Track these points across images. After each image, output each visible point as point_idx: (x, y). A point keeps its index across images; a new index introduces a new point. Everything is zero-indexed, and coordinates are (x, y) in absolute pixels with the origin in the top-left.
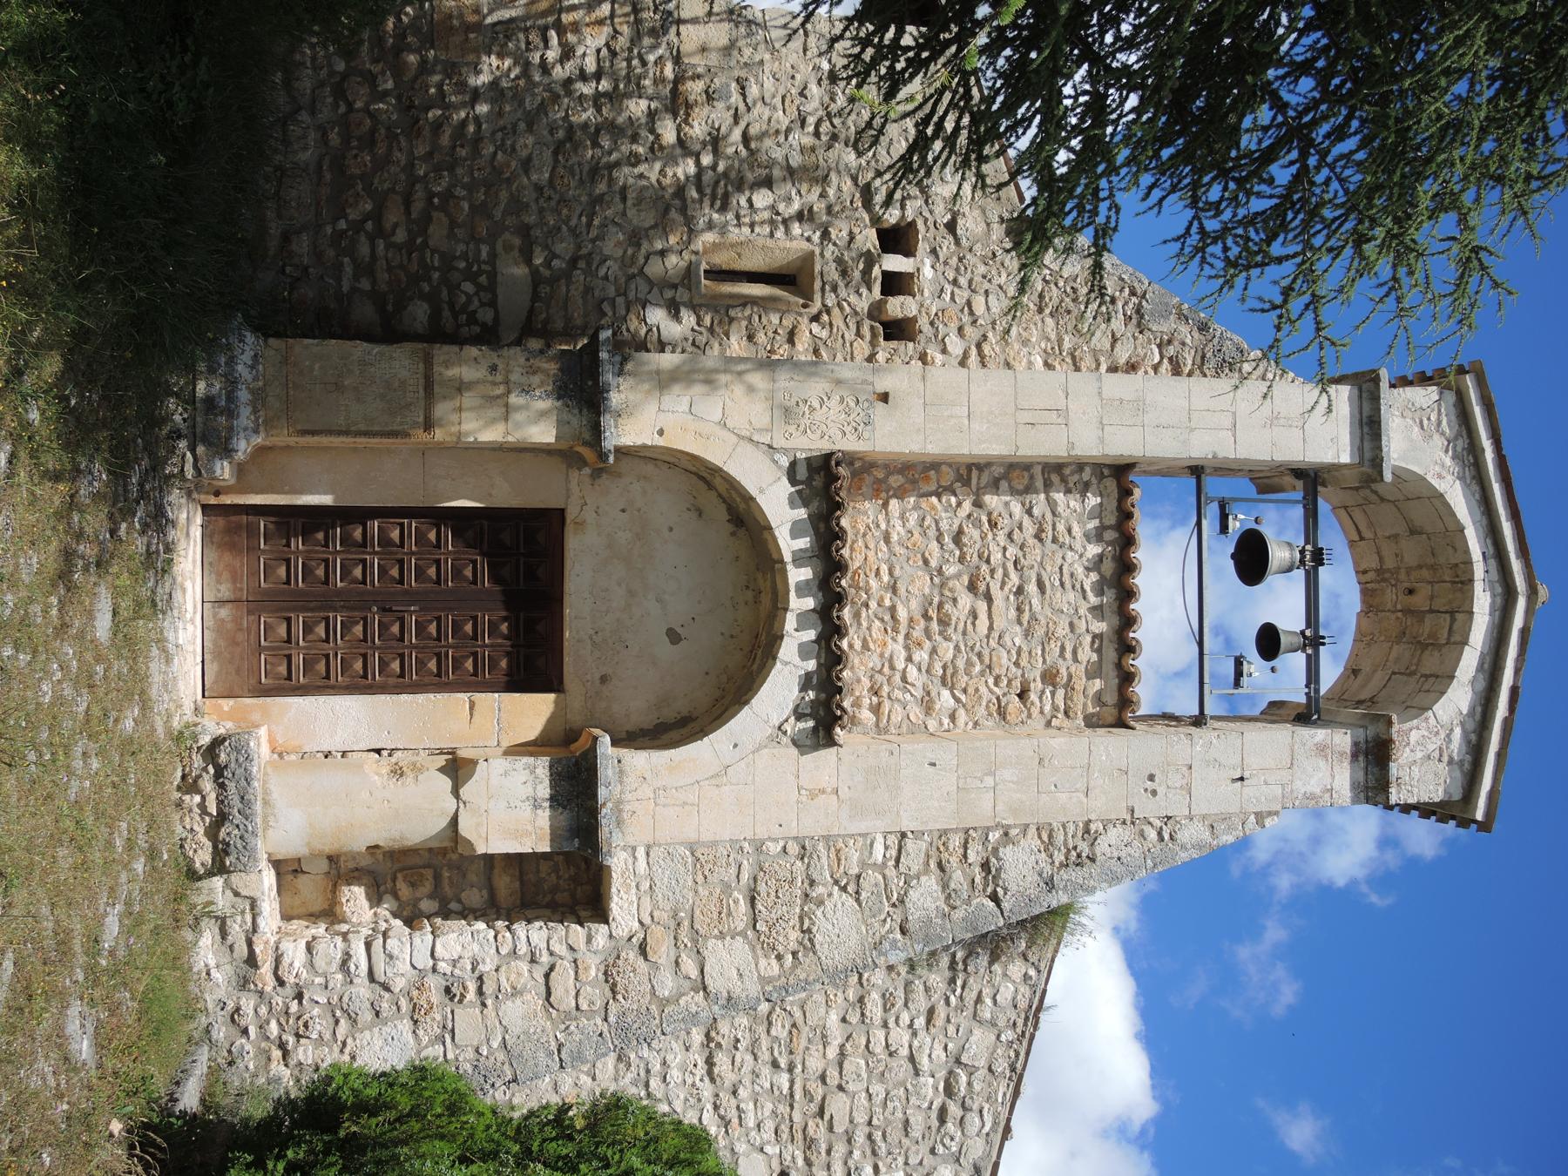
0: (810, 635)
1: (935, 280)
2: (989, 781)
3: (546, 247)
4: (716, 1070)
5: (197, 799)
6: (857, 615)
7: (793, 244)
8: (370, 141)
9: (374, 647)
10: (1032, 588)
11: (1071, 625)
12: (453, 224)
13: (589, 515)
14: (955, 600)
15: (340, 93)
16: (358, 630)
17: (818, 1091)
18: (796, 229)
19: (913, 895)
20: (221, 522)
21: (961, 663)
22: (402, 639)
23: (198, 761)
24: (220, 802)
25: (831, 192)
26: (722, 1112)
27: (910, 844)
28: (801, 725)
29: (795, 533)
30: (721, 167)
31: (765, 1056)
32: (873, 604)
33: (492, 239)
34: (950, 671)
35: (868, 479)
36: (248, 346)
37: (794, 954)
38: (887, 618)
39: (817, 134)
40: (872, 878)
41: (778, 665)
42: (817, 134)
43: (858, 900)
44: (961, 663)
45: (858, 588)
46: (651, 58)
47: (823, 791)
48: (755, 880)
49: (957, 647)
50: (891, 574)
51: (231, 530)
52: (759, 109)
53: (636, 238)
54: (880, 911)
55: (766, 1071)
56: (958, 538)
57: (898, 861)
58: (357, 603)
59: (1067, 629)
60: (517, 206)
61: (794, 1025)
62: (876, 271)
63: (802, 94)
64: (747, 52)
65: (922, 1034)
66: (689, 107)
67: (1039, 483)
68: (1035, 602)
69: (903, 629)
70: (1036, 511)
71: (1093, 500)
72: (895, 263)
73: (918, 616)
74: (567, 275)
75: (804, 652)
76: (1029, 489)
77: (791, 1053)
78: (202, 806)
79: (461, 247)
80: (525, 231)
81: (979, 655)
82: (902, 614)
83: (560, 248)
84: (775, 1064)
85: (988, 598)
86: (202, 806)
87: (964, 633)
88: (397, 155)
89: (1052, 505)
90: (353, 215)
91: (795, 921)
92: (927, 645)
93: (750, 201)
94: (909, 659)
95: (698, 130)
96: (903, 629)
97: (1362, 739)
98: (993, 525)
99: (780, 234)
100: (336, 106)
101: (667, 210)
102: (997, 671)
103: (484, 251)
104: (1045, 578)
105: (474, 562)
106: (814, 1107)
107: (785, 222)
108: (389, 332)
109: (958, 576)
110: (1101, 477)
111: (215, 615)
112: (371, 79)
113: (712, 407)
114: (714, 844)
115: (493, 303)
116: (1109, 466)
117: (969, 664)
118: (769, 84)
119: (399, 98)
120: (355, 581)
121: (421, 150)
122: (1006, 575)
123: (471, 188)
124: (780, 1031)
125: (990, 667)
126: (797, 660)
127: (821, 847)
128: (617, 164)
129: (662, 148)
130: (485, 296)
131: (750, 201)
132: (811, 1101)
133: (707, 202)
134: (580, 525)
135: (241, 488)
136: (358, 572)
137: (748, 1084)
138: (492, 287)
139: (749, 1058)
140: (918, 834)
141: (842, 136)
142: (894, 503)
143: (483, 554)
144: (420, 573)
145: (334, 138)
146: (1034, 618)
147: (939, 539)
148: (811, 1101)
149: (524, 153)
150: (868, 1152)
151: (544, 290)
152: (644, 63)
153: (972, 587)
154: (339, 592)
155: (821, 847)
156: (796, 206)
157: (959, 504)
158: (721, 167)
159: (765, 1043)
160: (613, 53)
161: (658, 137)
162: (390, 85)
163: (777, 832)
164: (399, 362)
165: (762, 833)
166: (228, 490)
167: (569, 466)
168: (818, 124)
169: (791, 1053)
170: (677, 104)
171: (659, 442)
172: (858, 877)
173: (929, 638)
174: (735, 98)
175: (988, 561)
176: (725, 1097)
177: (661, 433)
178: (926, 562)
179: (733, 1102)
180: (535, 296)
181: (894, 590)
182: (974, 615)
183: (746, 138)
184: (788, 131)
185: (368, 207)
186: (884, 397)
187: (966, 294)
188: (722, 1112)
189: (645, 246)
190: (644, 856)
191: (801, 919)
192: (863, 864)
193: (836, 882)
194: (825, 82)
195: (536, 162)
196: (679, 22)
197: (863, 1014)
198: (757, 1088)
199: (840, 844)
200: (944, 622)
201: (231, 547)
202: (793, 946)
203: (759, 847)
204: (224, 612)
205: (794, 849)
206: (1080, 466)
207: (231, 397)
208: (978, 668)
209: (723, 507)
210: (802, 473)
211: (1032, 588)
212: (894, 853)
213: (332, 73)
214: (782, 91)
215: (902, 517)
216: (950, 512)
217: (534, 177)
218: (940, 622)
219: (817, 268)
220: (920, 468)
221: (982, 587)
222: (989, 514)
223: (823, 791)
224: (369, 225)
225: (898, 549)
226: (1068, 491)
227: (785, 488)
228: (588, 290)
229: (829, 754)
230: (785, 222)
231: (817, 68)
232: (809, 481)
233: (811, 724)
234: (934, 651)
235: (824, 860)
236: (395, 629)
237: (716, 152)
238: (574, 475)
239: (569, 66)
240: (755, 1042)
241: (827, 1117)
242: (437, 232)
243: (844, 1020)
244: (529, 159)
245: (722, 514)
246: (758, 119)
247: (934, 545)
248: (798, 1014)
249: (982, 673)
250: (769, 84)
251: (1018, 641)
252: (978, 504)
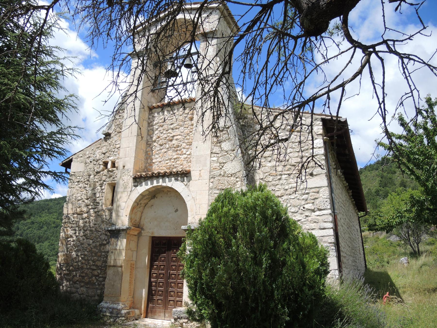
0: (167, 179)
1: (113, 157)
3: (103, 241)
4: (279, 195)
5: (184, 324)
6: (176, 167)
7: (106, 188)
8: (83, 277)
9: (177, 281)
10: (172, 126)
11: (180, 116)
12: (98, 260)
13: (151, 231)
14: (174, 144)
15: (75, 283)
16: (173, 284)
17: (288, 167)
18: (103, 187)
19: (225, 149)
20: (150, 314)
21: (186, 141)
22: (175, 274)
23: (177, 323)
24: (185, 319)
25: (97, 180)
26: (291, 193)
27: (214, 151)
28: (185, 180)
29: (147, 185)
30: (92, 204)
31: (277, 182)
32: (173, 164)
33: (101, 252)
34: (188, 144)
35: (149, 167)
36: (103, 304)
37: (237, 178)
38: (176, 160)
39: (87, 184)
40: (221, 160)
41: (172, 187)
42: (87, 184)
43: (225, 163)
44: (186, 141)
45: (170, 168)
46: (73, 220)
47: (200, 174)
48: (218, 189)
49: (183, 143)
50: (167, 160)
51: (151, 312)
52: (82, 197)
53: (103, 222)
54: (228, 157)
55: (281, 182)
56: (161, 145)
57: (217, 154)
58: (168, 285)
59: (181, 116)
60: (95, 247)
61: (269, 175)
62: (110, 170)
63: (81, 188)
64: (73, 200)
66: (81, 211)
67: (152, 128)
68: (175, 125)
69: (178, 156)
70: (157, 128)
71: (156, 115)
72: (109, 165)
73: (176, 153)
75: (170, 181)
76: (153, 130)
77: (277, 175)
78: (186, 323)
79: (102, 259)
80: (101, 245)
81: (185, 137)
82: (175, 157)
83: (103, 238)
84: (280, 179)
85: (173, 136)
86: (186, 323)
87: (180, 141)
88: (86, 272)
89: (156, 124)
90: (95, 281)
91: (229, 179)
92: (182, 150)
93: (98, 198)
94: (185, 154)
95: (85, 209)
96: (178, 156)
97: (202, 40)
98: (159, 137)
99: (104, 191)
100: (77, 284)
101: (98, 215)
102: (189, 132)
103: (103, 254)
104: (170, 123)
105: (161, 257)
106: (293, 168)
107: (102, 190)
109: (169, 144)
110: (152, 113)
111: (167, 317)
112: (74, 276)
113: (123, 205)
114: (209, 200)
116: (150, 112)
117: (187, 139)
118: (79, 195)
119: (77, 271)
120: (163, 285)
121: (85, 267)
122: (169, 133)
123: (92, 256)
124: (270, 179)
125: (188, 134)
126: (172, 182)
127: (212, 173)
128: (90, 226)
129: (88, 217)
131: (98, 198)
132: (291, 169)
133: (97, 207)
134: (152, 233)
135: (140, 309)
136: (161, 284)
137: (284, 186)
139: (277, 187)
140: (212, 149)
141: (88, 179)
142: (153, 161)
143: (160, 255)
144: (162, 270)
145: (82, 284)
146: (178, 125)
147: (161, 149)
148: (291, 169)
149: (87, 245)
150: (307, 151)
152: (74, 221)
153: (171, 141)
154: (165, 289)
155: (212, 173)
156: (99, 188)
157: (155, 146)
158: (92, 204)
159: (274, 182)
160: (72, 227)
161: (86, 217)
162: (75, 273)
163: (208, 185)
164: (110, 272)
165: (208, 188)
166: (141, 311)
167: (141, 235)
168: (86, 184)
169: (277, 175)
170: (80, 214)
171: (128, 216)
172: (220, 163)
173: (181, 149)
174: (80, 202)
175: (166, 137)
176: (288, 192)
177: (126, 216)
178: (166, 152)
179: (289, 190)
181: (171, 159)
182: (177, 139)
183: (87, 199)
184: (87, 190)
185: (94, 278)
186: (124, 166)
187: (116, 149)
188: (291, 193)
189: (105, 220)
190: (323, 211)
191: (228, 177)
192: (217, 162)
193: (221, 169)
194: (79, 183)
195: (88, 243)
196: (68, 214)
197: (269, 157)
198: (286, 184)
199: (212, 168)
200: (178, 146)
201: (155, 312)
202: (235, 179)
203: (211, 189)
204: (167, 315)
205: (212, 180)
206: (149, 118)
207: (110, 308)
208: (188, 137)
209: (152, 200)
210: (136, 184)
211: (172, 126)
212: (216, 155)
213: (72, 284)
214: (80, 192)
215: (156, 159)
216: (156, 146)
217: (91, 243)
218: (178, 147)
219: (110, 182)
220: (147, 156)
221: (171, 138)
222: (157, 138)
223: (200, 174)
224: (97, 278)
225: (162, 159)
226: (154, 121)
227: (139, 188)
229: (192, 173)
230: (102, 190)
231: (77, 185)
232: (138, 182)
233: (185, 178)
234: (184, 148)
235: (215, 172)
236: (173, 276)
237: (89, 205)
238: (143, 234)
239: (74, 236)
240: (273, 185)
241: (295, 164)
243: (270, 162)
244: (88, 244)
245: (152, 201)
246: (84, 197)
247: (162, 151)
248: (267, 174)
249: (189, 136)
250: (79, 195)
251: (183, 128)
252: (155, 141)
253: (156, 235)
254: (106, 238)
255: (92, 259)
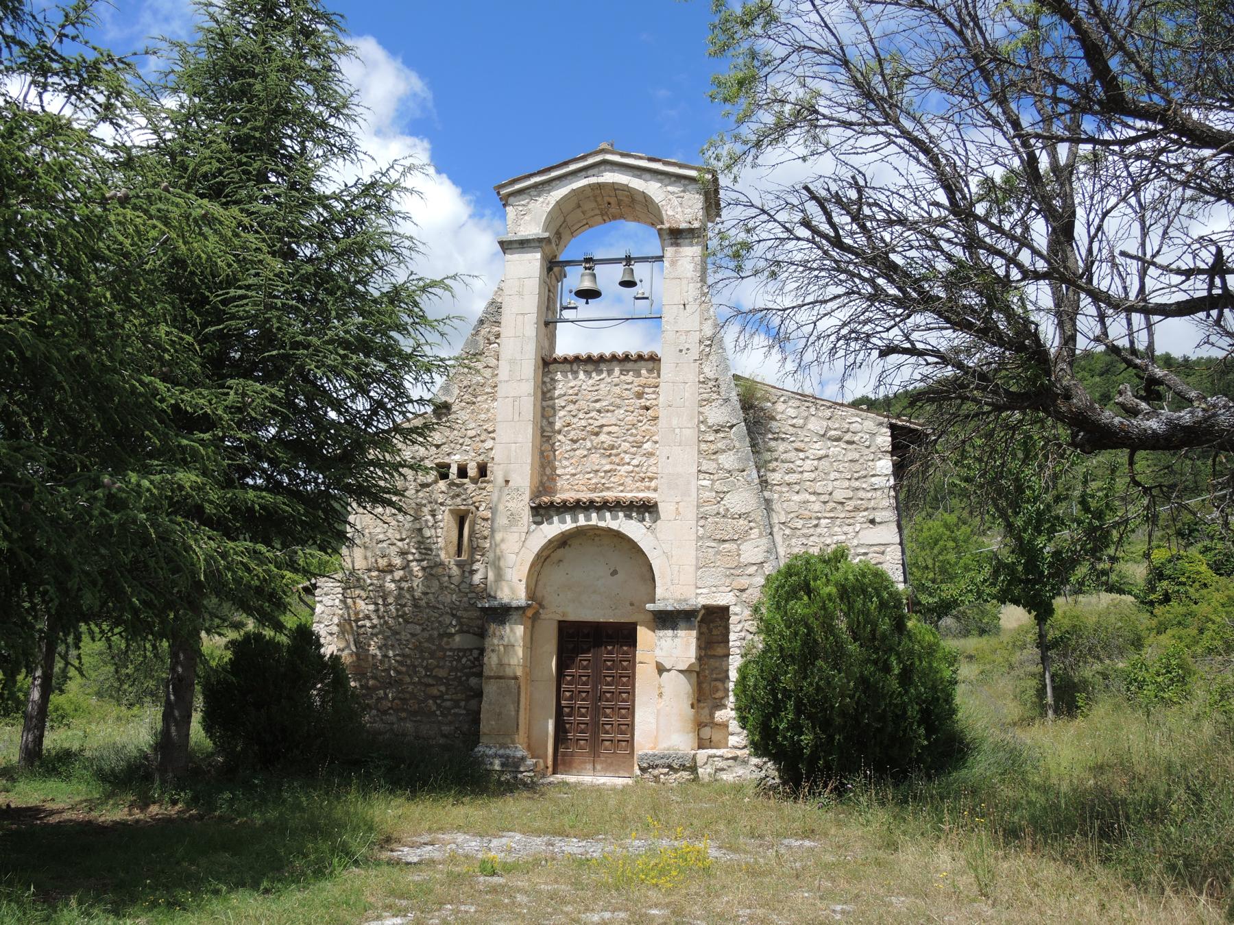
0: (608, 515)
2: (677, 431)
7: (446, 519)
8: (404, 700)
10: (598, 405)
12: (438, 666)
15: (385, 712)
17: (832, 505)
18: (440, 517)
19: (727, 466)
20: (560, 768)
21: (631, 439)
23: (647, 776)
27: (703, 468)
29: (563, 522)
31: (811, 531)
33: (444, 650)
35: (547, 484)
36: (480, 749)
40: (717, 486)
44: (631, 439)
51: (564, 763)
53: (442, 588)
55: (819, 530)
56: (574, 441)
58: (597, 711)
60: (430, 639)
62: (458, 481)
65: (807, 454)
67: (550, 403)
69: (614, 467)
74: (459, 619)
75: (615, 518)
76: (553, 408)
78: (665, 774)
80: (441, 636)
82: (608, 467)
83: (448, 622)
84: (816, 526)
85: (602, 426)
86: (665, 774)
90: (434, 708)
91: (735, 522)
95: (398, 561)
96: (614, 467)
98: (569, 425)
99: (441, 524)
103: (448, 653)
106: (839, 507)
108: (479, 694)
109: (591, 441)
110: (549, 372)
112: (379, 699)
113: (510, 559)
114: (697, 558)
115: (471, 650)
117: (631, 435)
118: (378, 530)
121: (408, 679)
123: (423, 659)
130: (468, 653)
135: (545, 758)
136: (583, 710)
138: (464, 650)
140: (699, 464)
142: (558, 472)
145: (403, 715)
146: (611, 404)
147: (574, 450)
151: (465, 628)
153: (597, 434)
156: (429, 517)
159: (805, 531)
163: (694, 530)
164: (490, 689)
165: (694, 537)
166: (545, 762)
170: (390, 569)
171: (524, 581)
174: (385, 545)
180: (468, 632)
183: (402, 540)
192: (711, 490)
200: (612, 447)
202: (746, 522)
203: (699, 538)
204: (598, 767)
205: (702, 522)
206: (544, 383)
207: (501, 756)
210: (539, 519)
211: (598, 405)
215: (565, 468)
216: (563, 444)
227: (545, 526)
228: (465, 609)
229: (661, 507)
232: (542, 516)
234: (625, 452)
236: (608, 695)
237: (407, 553)
238: (543, 616)
242: (442, 673)
245: (561, 552)
247: (577, 453)
250: (378, 530)
252: (559, 432)
253: (572, 617)
254: (454, 623)
255: (425, 663)
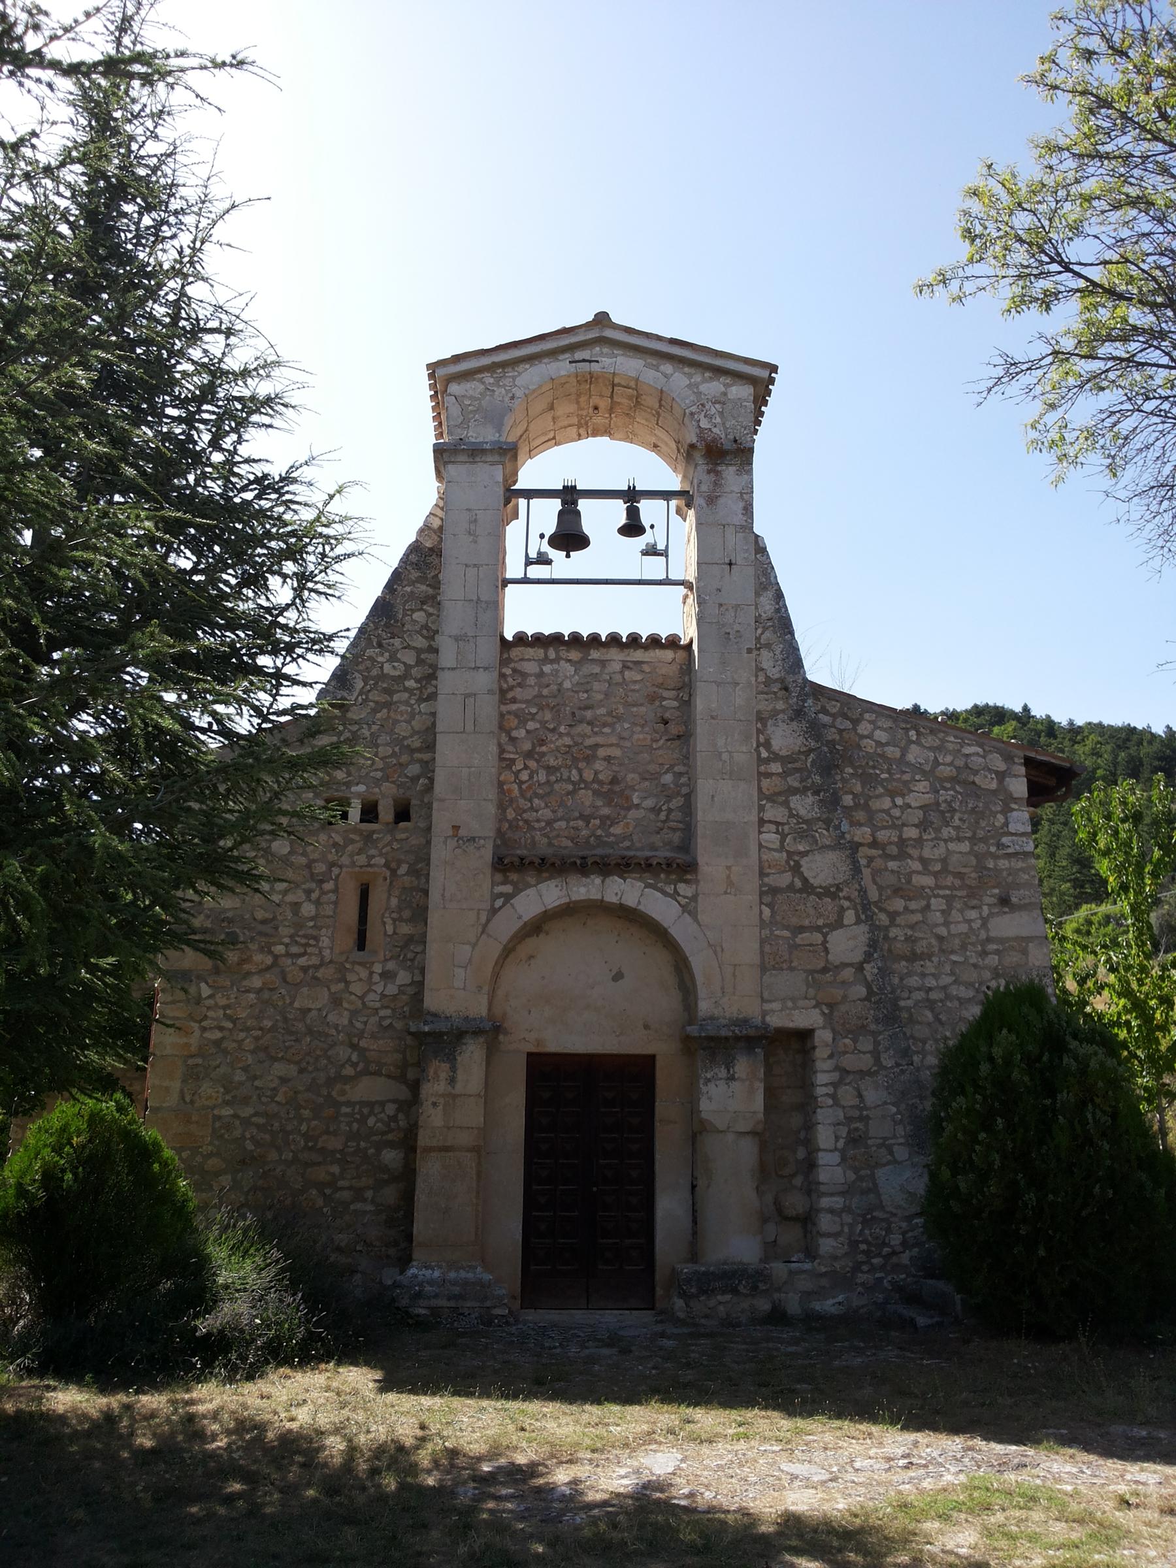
2: (725, 756)
3: (343, 1066)
12: (327, 1132)
35: (509, 834)
41: (641, 907)
65: (908, 800)
74: (362, 1051)
90: (320, 1202)
101: (317, 979)
103: (345, 1110)
108: (407, 1176)
115: (383, 1104)
116: (501, 653)
130: (377, 1109)
134: (539, 1042)
138: (371, 1105)
151: (373, 1068)
163: (756, 910)
180: (377, 1073)
182: (608, 759)
185: (314, 1192)
228: (373, 1036)
242: (335, 1143)
253: (553, 1046)
254: (354, 1058)
255: (304, 1128)
